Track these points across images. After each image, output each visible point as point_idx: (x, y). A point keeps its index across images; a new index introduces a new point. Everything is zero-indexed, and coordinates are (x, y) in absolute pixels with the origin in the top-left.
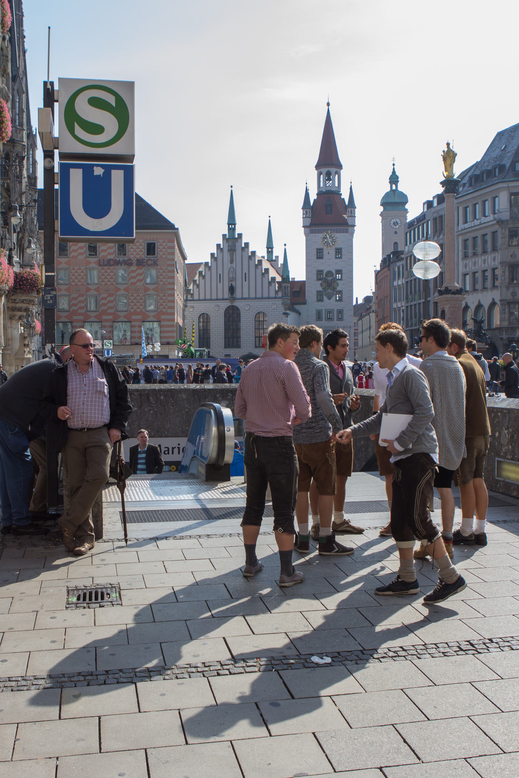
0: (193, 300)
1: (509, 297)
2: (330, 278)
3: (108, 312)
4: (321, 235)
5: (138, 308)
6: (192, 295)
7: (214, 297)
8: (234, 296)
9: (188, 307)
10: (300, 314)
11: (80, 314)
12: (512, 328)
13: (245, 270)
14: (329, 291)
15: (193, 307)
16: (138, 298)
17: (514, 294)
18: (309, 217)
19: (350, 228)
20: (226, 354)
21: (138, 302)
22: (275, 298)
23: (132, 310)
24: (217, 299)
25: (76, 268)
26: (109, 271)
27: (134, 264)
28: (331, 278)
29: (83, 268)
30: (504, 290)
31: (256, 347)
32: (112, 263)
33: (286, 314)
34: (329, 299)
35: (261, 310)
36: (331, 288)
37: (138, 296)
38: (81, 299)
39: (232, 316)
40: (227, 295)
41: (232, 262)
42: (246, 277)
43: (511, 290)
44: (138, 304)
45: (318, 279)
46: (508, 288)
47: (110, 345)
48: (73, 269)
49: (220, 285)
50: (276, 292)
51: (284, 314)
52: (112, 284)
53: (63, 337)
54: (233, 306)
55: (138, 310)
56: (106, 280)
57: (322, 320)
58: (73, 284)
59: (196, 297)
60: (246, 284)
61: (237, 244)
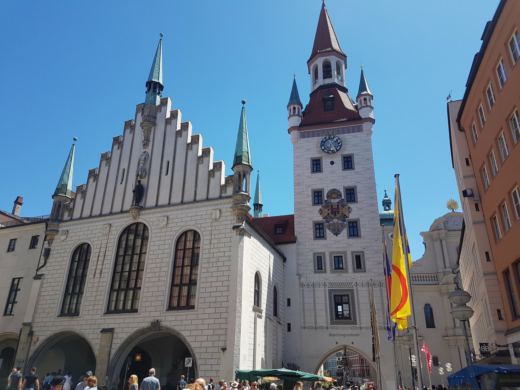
0: (71, 220)
2: (335, 201)
4: (316, 140)
8: (142, 204)
9: (60, 233)
10: (284, 259)
18: (298, 115)
19: (365, 125)
20: (106, 327)
28: (337, 200)
41: (146, 144)
42: (169, 168)
45: (315, 204)
49: (120, 188)
51: (235, 228)
54: (137, 224)
59: (76, 214)
60: (166, 180)
61: (159, 115)
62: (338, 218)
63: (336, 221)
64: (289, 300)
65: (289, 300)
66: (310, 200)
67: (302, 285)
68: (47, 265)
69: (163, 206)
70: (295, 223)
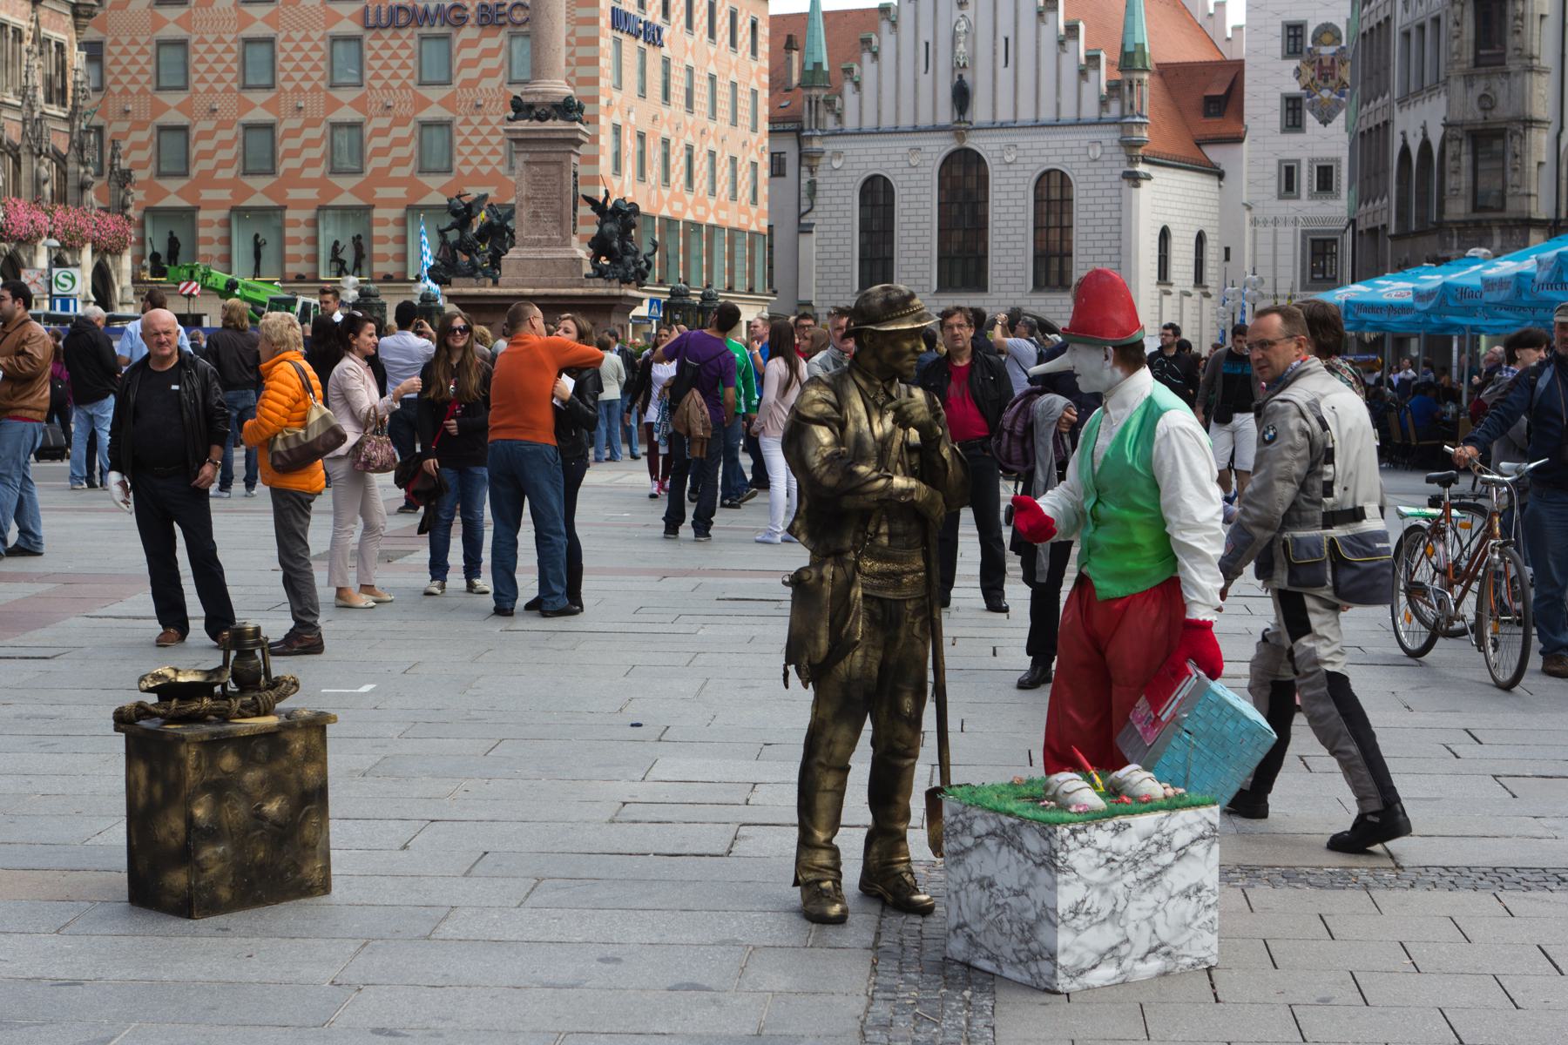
0: (842, 133)
1: (1471, 113)
2: (1327, 51)
3: (392, 175)
5: (485, 162)
6: (839, 117)
7: (906, 121)
8: (968, 118)
9: (828, 153)
10: (1221, 176)
11: (310, 184)
12: (1478, 223)
13: (1005, 29)
14: (1326, 93)
15: (838, 154)
16: (485, 130)
17: (1487, 102)
21: (485, 142)
22: (1099, 122)
23: (466, 170)
24: (916, 130)
25: (297, 36)
26: (395, 43)
27: (472, 20)
29: (316, 36)
30: (1458, 86)
31: (1038, 286)
32: (403, 19)
33: (1134, 179)
34: (1325, 122)
35: (1054, 163)
36: (1332, 83)
37: (485, 122)
38: (310, 133)
39: (964, 183)
40: (945, 115)
43: (1480, 87)
44: (485, 150)
46: (1469, 79)
47: (69, 283)
48: (288, 39)
49: (925, 81)
50: (1104, 103)
52: (404, 86)
53: (258, 256)
55: (485, 170)
56: (386, 74)
57: (1298, 197)
58: (289, 86)
59: (850, 123)
60: (1005, 75)
62: (1331, 89)
63: (1326, 93)
64: (1227, 250)
65: (1227, 250)
66: (1276, 45)
67: (1254, 222)
68: (816, 208)
69: (1003, 126)
70: (1246, 97)
